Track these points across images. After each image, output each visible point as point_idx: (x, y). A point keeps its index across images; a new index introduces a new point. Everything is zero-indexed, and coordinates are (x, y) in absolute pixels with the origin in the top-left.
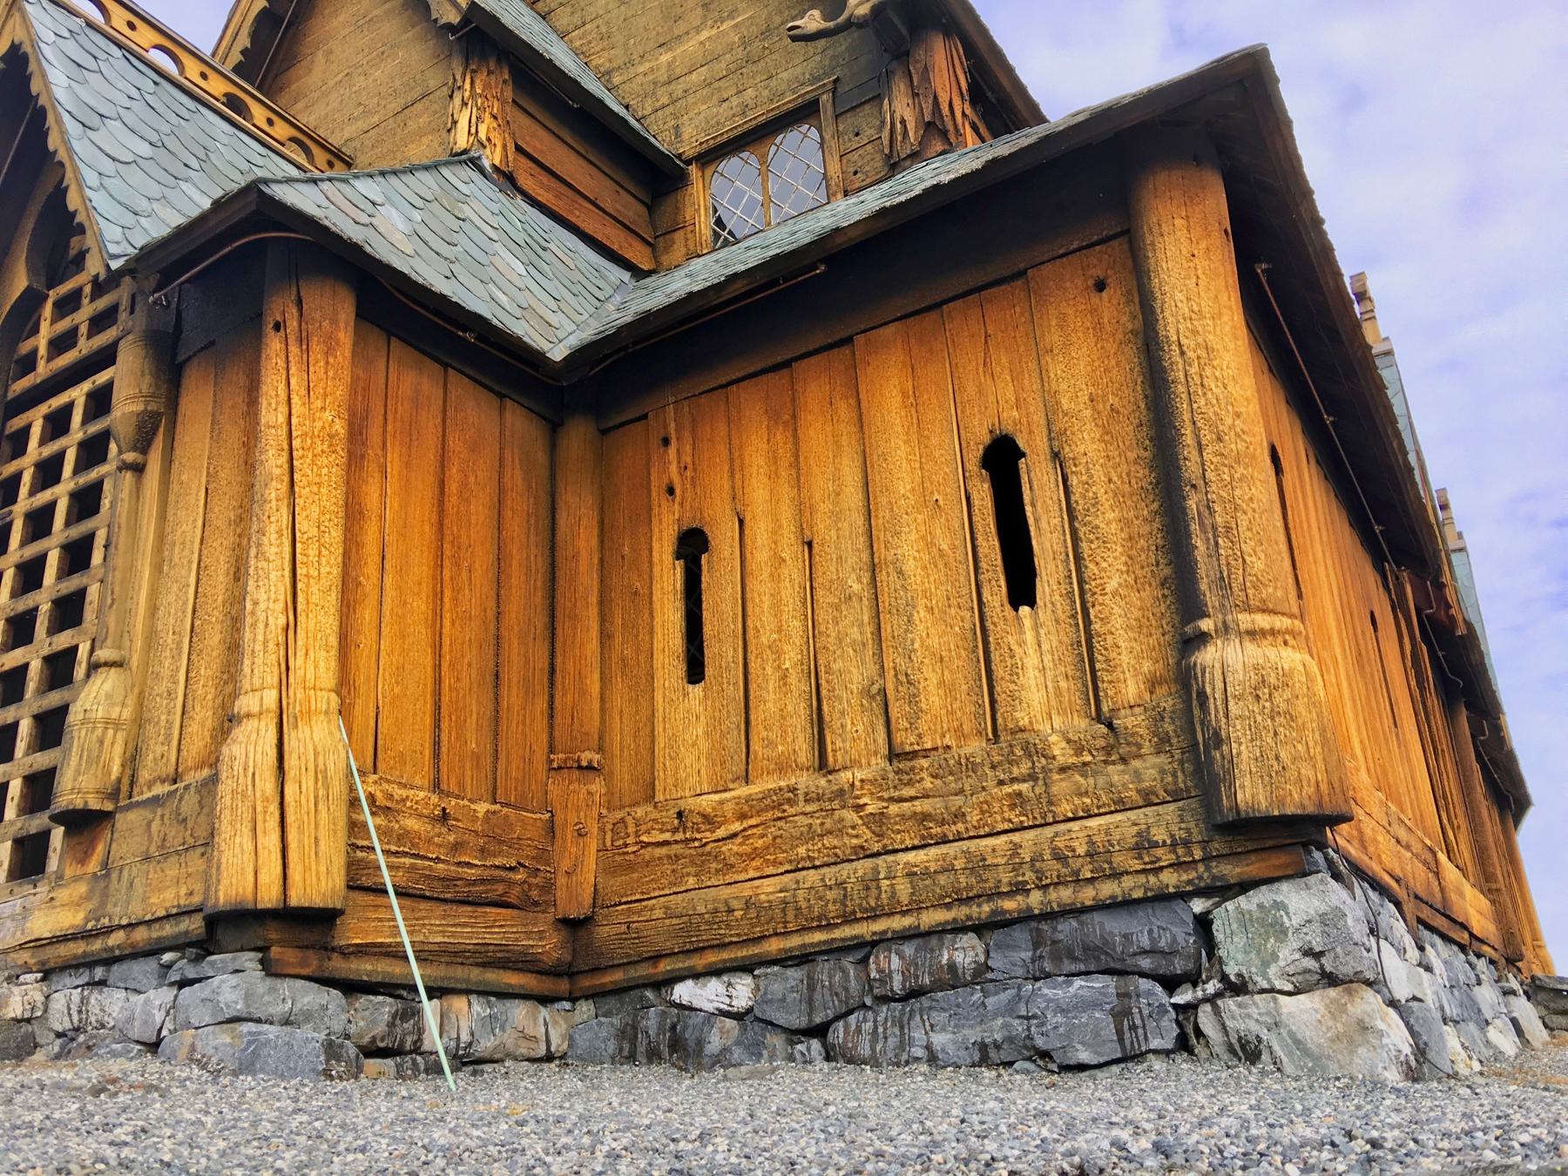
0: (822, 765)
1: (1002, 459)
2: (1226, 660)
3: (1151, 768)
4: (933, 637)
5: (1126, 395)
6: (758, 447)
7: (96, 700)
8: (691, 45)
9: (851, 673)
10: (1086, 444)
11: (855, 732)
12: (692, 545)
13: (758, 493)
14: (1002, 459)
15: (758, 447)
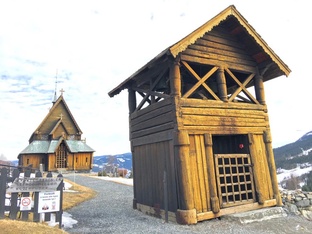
0: (80, 165)
1: (87, 158)
2: (91, 165)
3: (89, 167)
4: (84, 163)
5: (90, 157)
6: (80, 156)
7: (68, 163)
8: (69, 128)
9: (82, 163)
10: (89, 158)
11: (81, 165)
12: (77, 158)
13: (79, 157)
14: (87, 158)
15: (80, 156)
